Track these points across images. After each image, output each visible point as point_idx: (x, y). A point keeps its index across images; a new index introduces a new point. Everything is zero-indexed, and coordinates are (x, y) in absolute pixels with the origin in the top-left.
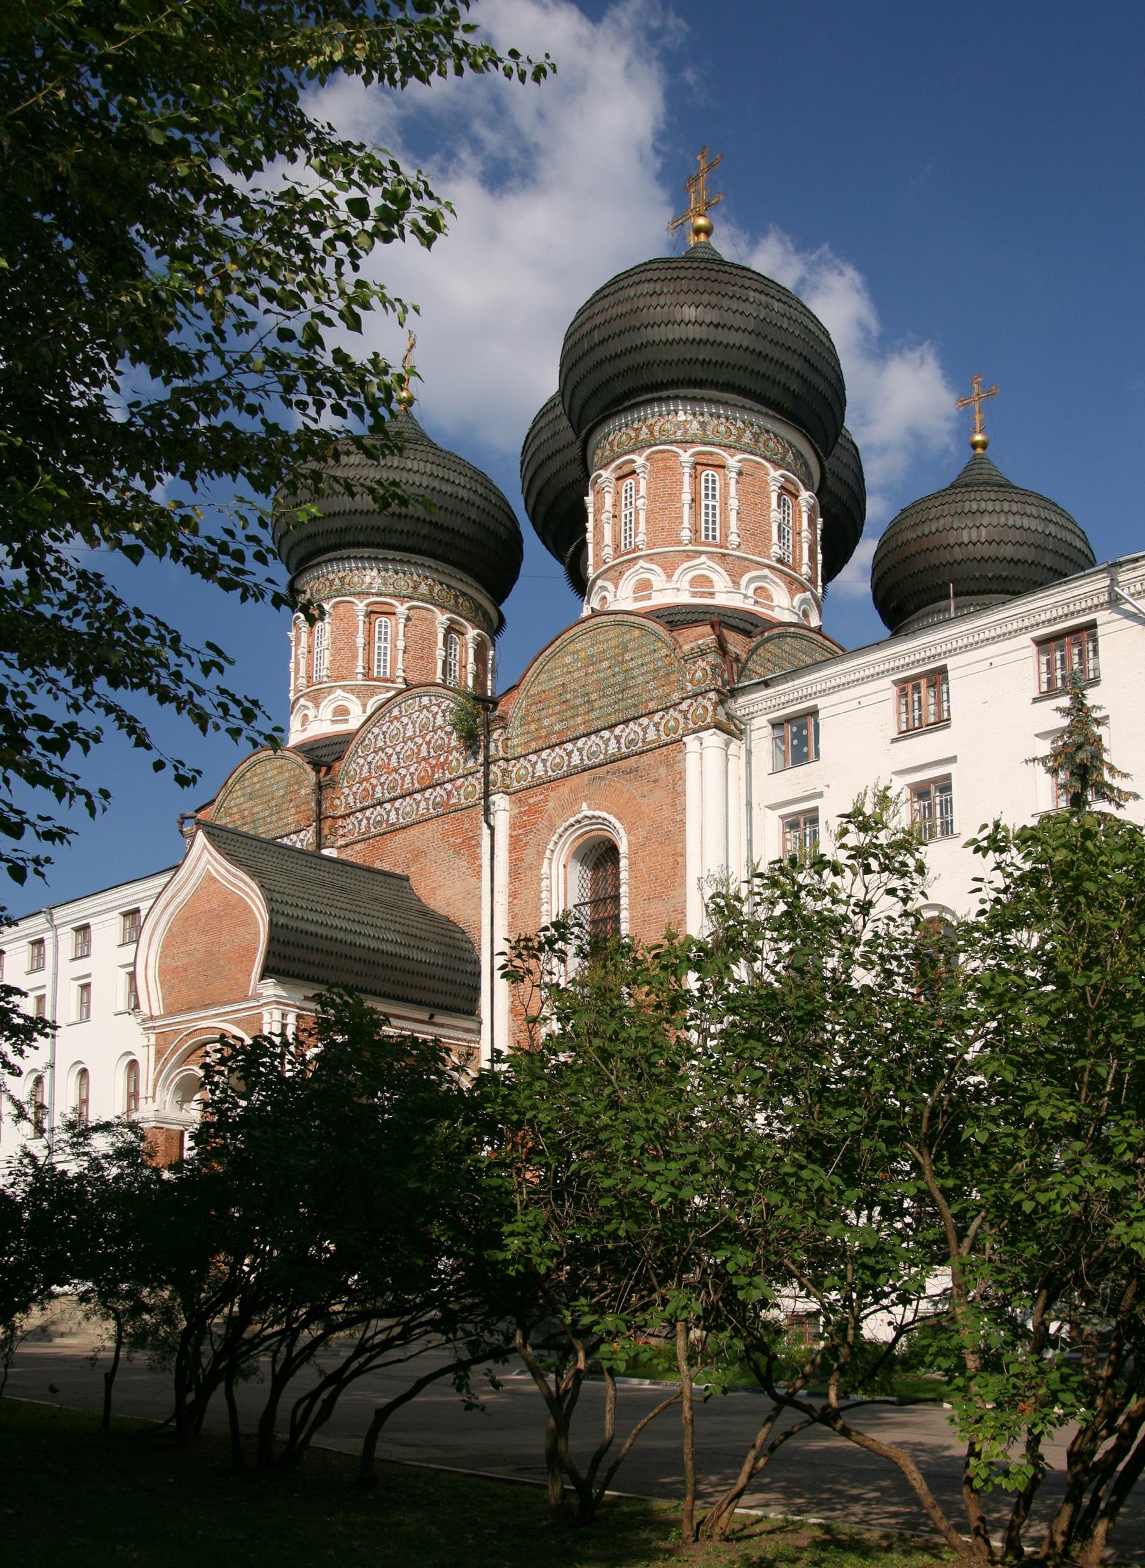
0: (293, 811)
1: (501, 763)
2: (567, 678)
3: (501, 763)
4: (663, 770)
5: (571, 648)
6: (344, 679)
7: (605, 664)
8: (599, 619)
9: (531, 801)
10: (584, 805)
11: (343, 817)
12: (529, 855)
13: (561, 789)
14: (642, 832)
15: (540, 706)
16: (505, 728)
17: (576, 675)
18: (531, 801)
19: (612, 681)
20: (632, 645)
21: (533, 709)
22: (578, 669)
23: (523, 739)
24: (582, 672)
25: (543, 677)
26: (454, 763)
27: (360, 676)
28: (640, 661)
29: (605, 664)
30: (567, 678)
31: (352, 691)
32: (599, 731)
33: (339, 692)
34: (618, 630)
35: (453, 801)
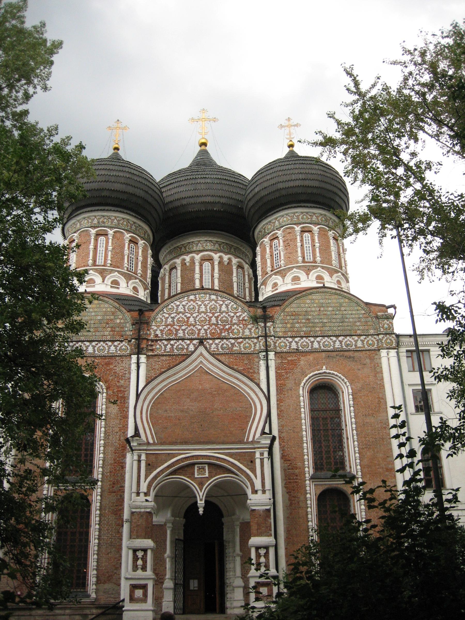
0: (109, 329)
1: (273, 338)
2: (309, 309)
3: (273, 338)
4: (368, 361)
5: (310, 297)
6: (118, 267)
7: (330, 309)
8: (326, 290)
9: (289, 359)
10: (324, 367)
11: (152, 341)
12: (290, 384)
13: (308, 357)
14: (359, 385)
15: (293, 317)
16: (273, 322)
17: (313, 309)
18: (289, 359)
19: (335, 316)
20: (344, 304)
21: (288, 318)
22: (314, 307)
23: (283, 330)
24: (318, 309)
25: (293, 305)
26: (236, 331)
27: (126, 269)
28: (350, 312)
29: (330, 309)
30: (309, 309)
31: (122, 275)
32: (331, 336)
33: (116, 273)
34: (336, 296)
35: (235, 348)
